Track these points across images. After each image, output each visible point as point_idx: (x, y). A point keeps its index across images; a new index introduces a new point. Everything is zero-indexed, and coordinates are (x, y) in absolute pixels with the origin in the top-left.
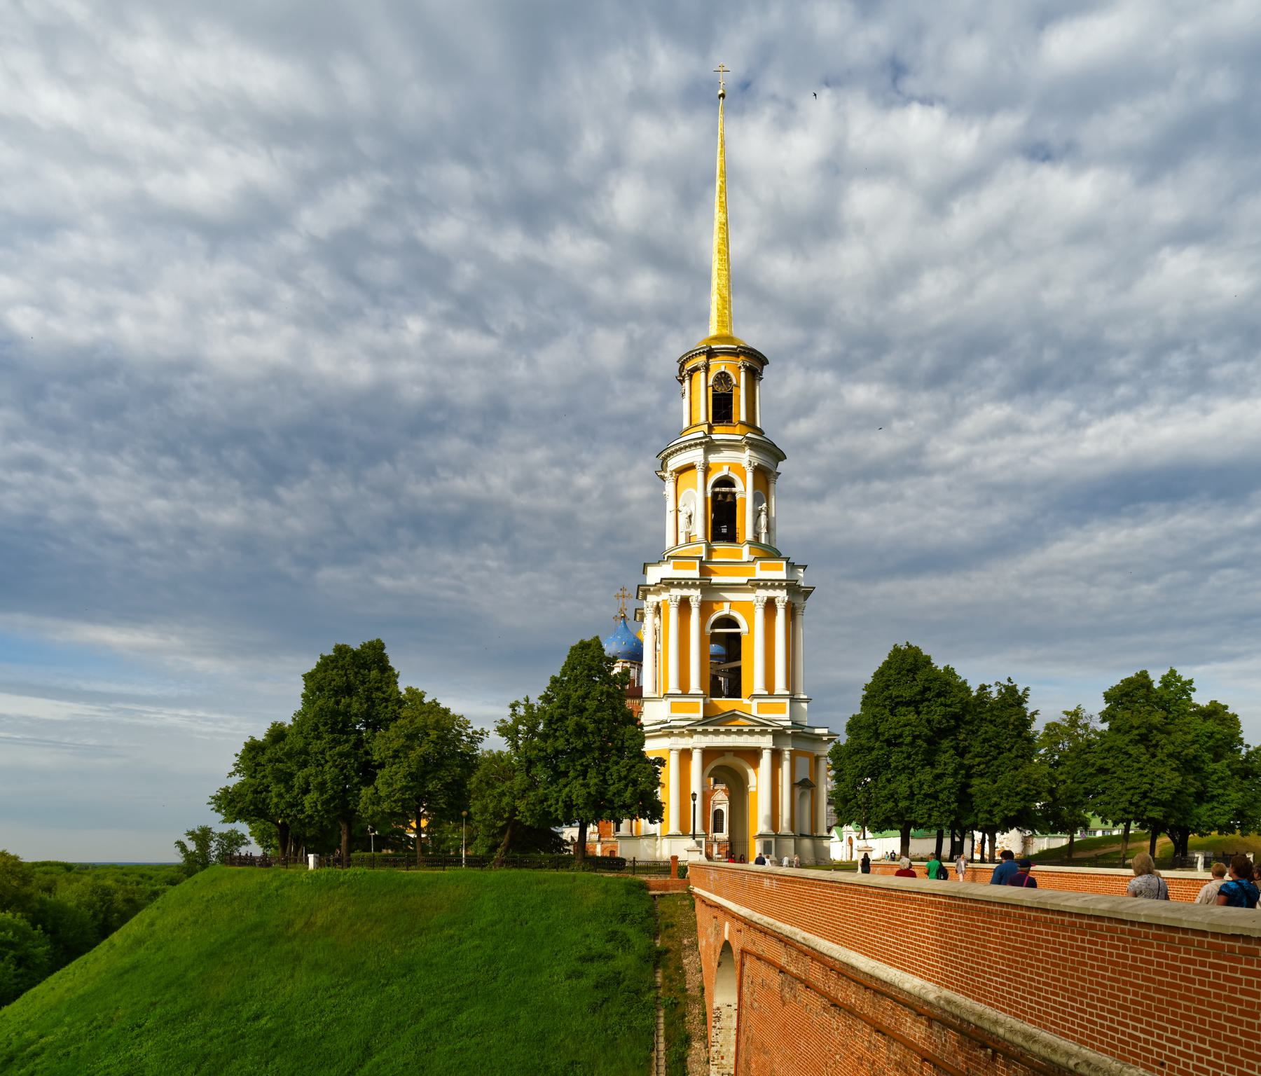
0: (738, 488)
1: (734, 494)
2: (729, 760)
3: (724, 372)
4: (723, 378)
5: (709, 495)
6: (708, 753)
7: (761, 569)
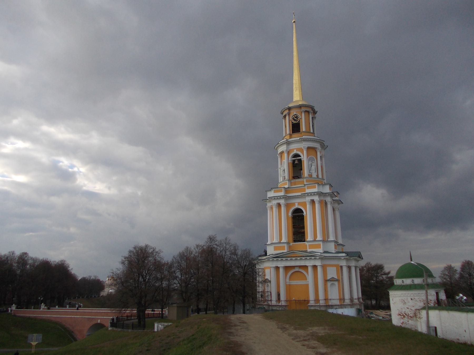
0: (302, 157)
2: (297, 269)
6: (287, 268)
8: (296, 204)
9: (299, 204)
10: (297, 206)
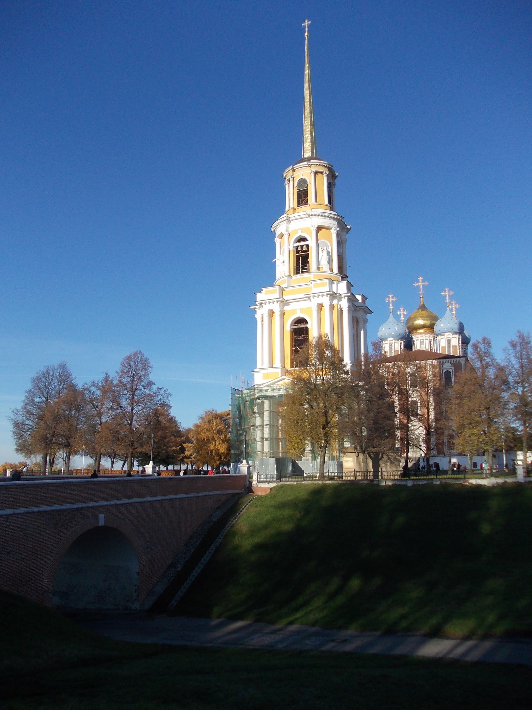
1: (307, 246)
3: (302, 178)
4: (303, 182)
5: (291, 248)
7: (314, 288)
8: (298, 311)
9: (302, 310)
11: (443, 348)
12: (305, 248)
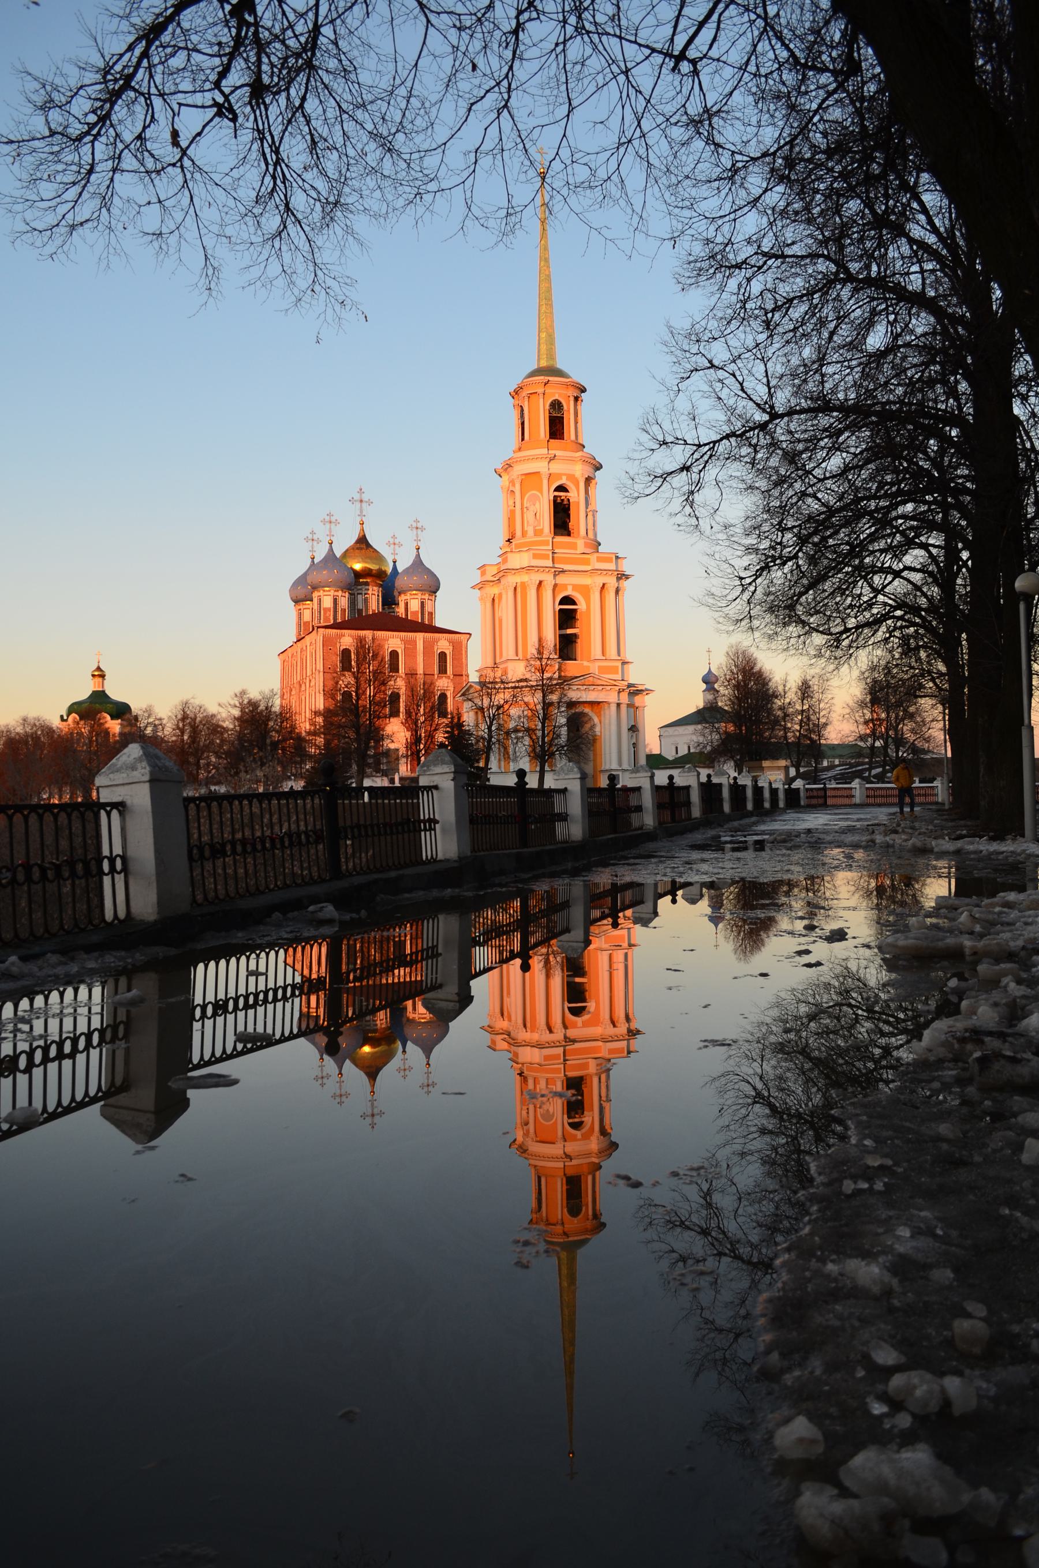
4: (556, 405)
5: (552, 498)
8: (570, 588)
9: (575, 587)
10: (569, 592)
11: (415, 613)
12: (565, 502)
